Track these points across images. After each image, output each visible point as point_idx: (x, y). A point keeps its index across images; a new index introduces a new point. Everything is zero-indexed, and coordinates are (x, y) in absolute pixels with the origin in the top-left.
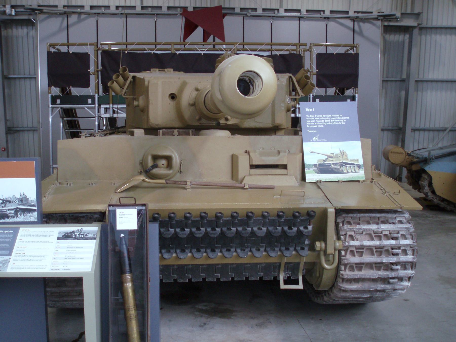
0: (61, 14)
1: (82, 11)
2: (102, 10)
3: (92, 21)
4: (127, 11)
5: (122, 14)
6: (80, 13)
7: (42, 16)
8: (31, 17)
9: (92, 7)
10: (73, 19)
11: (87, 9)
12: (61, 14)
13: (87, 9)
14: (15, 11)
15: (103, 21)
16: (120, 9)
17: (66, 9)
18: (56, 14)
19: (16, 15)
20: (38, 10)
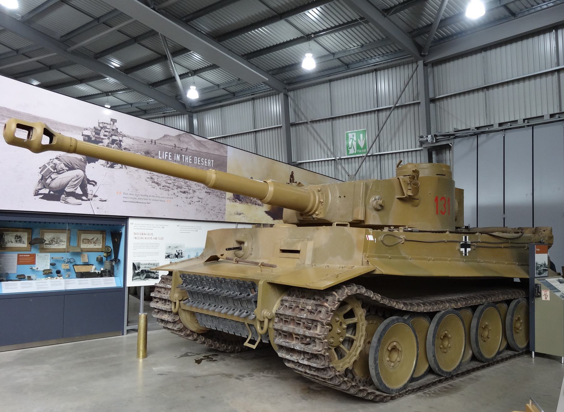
0: (471, 135)
1: (491, 129)
2: (508, 126)
3: (499, 136)
4: (532, 122)
5: (528, 126)
6: (491, 132)
7: (457, 140)
8: (448, 142)
9: (500, 125)
10: (482, 138)
11: (496, 127)
12: (471, 135)
13: (496, 127)
14: (436, 139)
15: (509, 135)
16: (526, 121)
17: (476, 131)
18: (466, 136)
19: (436, 142)
20: (454, 136)
